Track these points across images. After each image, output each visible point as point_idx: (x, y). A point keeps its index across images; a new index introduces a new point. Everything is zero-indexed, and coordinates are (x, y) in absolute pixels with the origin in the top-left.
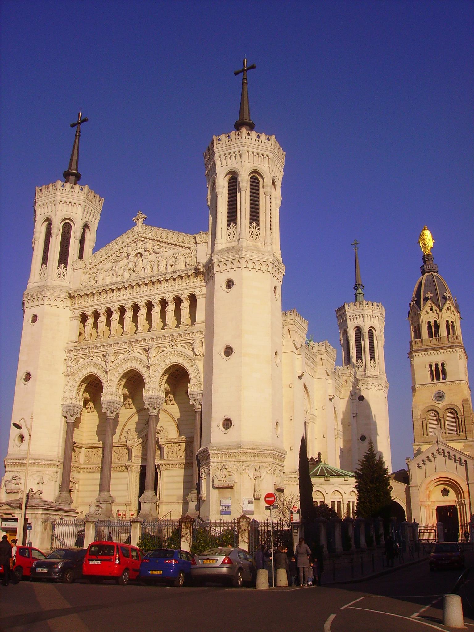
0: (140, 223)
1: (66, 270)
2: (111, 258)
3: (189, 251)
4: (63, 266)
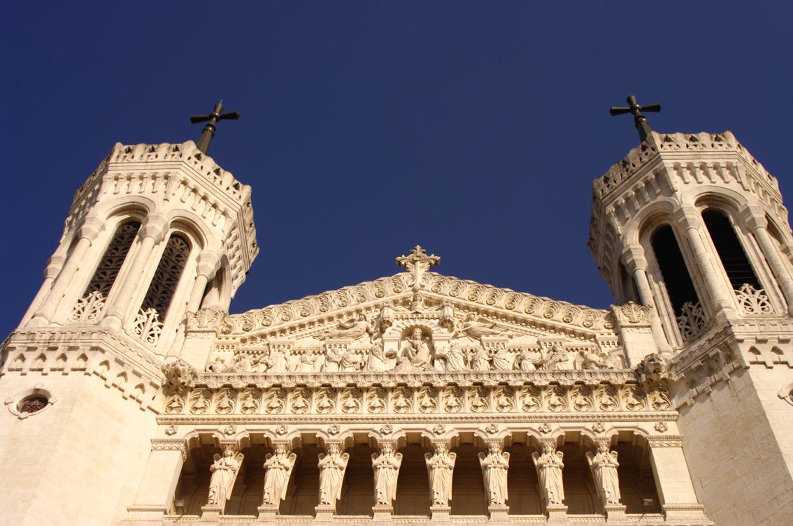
0: (420, 270)
1: (161, 327)
2: (317, 328)
3: (588, 343)
4: (153, 312)
